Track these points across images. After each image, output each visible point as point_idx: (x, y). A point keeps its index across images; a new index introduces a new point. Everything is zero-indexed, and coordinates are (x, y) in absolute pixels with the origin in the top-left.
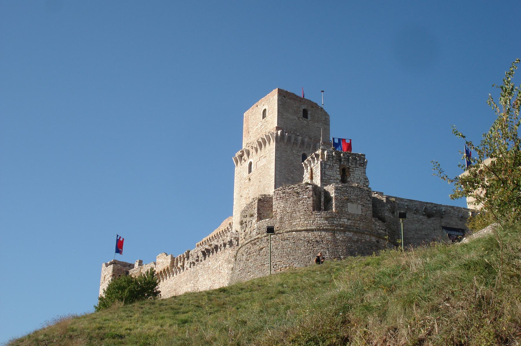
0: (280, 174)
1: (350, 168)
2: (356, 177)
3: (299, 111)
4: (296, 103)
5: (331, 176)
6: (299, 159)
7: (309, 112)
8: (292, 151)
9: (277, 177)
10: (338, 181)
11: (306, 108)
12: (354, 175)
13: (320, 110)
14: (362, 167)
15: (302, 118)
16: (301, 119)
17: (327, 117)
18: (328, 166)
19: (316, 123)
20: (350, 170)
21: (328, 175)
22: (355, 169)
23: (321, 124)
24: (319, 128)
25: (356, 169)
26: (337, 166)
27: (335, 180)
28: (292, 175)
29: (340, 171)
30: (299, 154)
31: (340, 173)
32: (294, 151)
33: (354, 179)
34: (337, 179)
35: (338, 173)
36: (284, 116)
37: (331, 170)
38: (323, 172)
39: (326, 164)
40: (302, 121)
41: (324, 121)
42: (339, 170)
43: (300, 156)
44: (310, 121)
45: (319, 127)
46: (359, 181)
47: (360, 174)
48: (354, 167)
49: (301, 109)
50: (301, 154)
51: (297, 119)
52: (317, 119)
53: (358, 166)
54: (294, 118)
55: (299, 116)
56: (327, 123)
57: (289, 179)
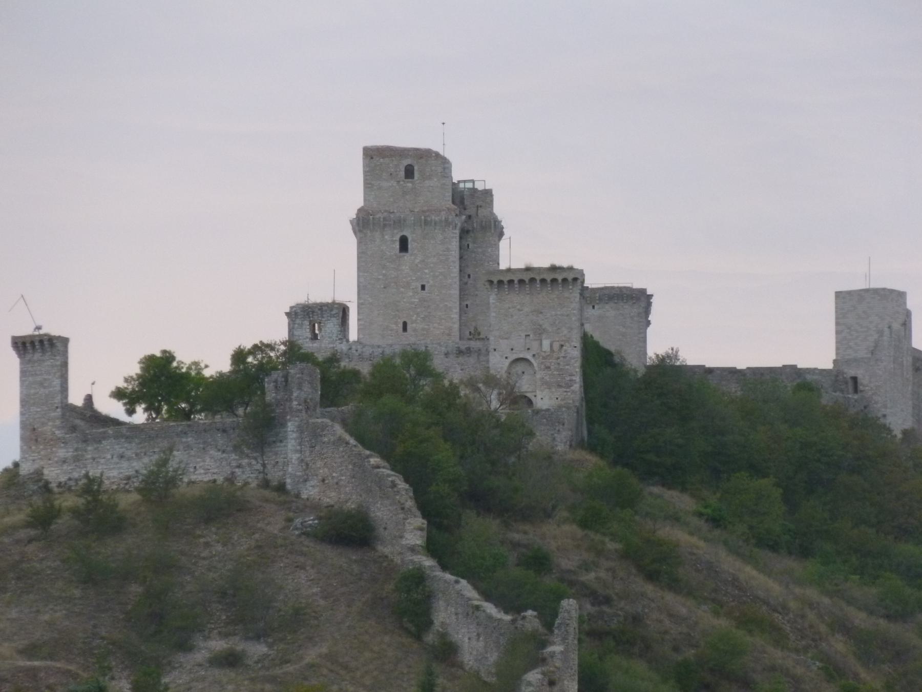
0: (366, 274)
1: (322, 322)
2: (328, 331)
3: (399, 171)
4: (393, 160)
5: (299, 336)
6: (394, 246)
7: (416, 168)
8: (383, 236)
9: (362, 280)
10: (308, 340)
11: (409, 163)
12: (326, 329)
13: (433, 158)
14: (335, 319)
15: (403, 181)
16: (402, 183)
17: (447, 165)
18: (296, 325)
19: (427, 182)
20: (322, 324)
21: (296, 336)
22: (326, 322)
23: (435, 180)
24: (432, 186)
25: (329, 322)
26: (307, 323)
27: (305, 339)
28: (384, 272)
29: (310, 329)
30: (394, 239)
31: (310, 331)
32: (386, 237)
33: (326, 334)
34: (307, 338)
35: (308, 330)
36: (375, 187)
37: (299, 330)
38: (291, 333)
39: (295, 324)
40: (404, 185)
41: (441, 172)
42: (308, 327)
43: (397, 240)
44: (417, 180)
45: (432, 185)
46: (331, 335)
47: (333, 326)
48: (326, 321)
49: (401, 167)
50: (397, 238)
51: (395, 184)
52: (428, 174)
53: (329, 318)
54: (390, 184)
55: (398, 180)
56: (446, 175)
57: (379, 279)
